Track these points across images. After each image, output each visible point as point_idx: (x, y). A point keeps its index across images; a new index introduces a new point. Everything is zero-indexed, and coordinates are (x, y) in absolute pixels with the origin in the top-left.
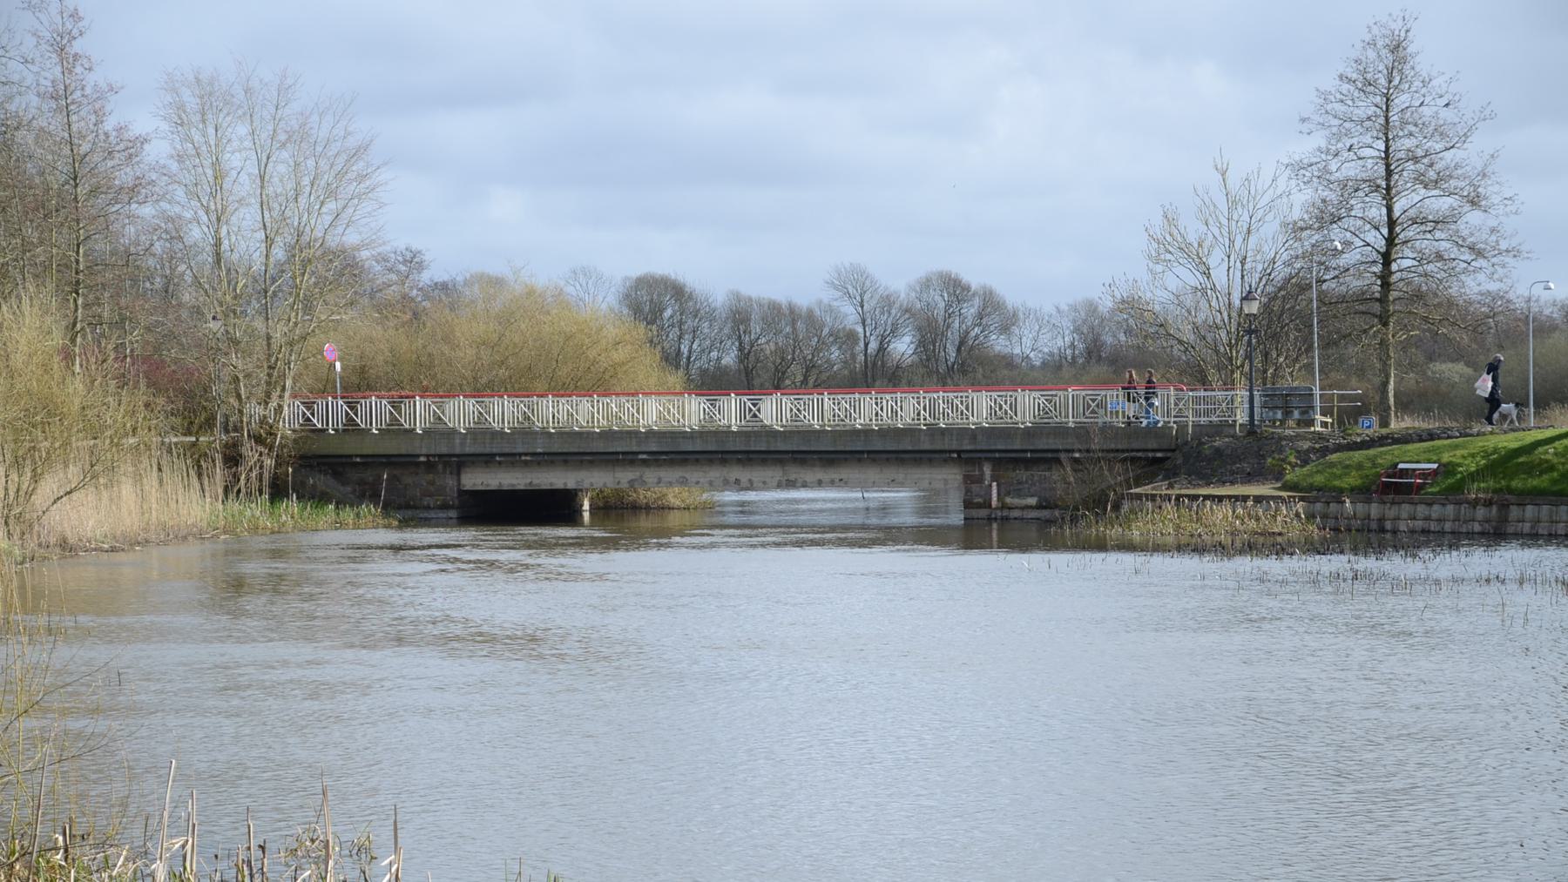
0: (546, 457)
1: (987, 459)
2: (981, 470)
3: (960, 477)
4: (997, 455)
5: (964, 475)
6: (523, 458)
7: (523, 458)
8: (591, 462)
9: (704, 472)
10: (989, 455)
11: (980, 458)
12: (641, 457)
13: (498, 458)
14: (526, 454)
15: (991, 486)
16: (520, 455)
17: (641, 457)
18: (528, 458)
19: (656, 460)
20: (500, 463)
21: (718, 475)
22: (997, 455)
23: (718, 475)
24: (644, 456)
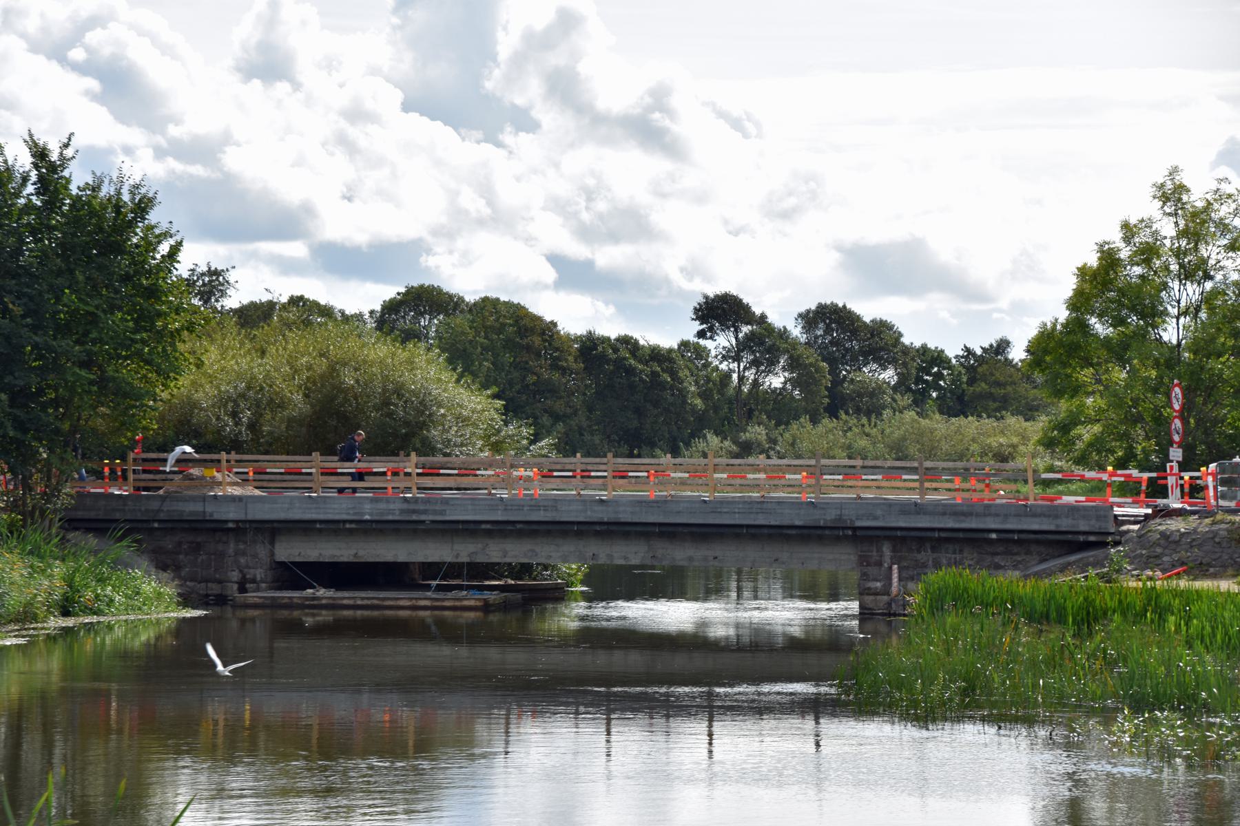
0: (374, 526)
1: (887, 538)
2: (879, 550)
3: (854, 558)
4: (899, 533)
5: (860, 556)
6: (348, 526)
7: (348, 526)
8: (770, 536)
9: (557, 545)
10: (888, 533)
11: (878, 537)
12: (483, 526)
13: (318, 526)
14: (351, 522)
15: (890, 568)
16: (345, 522)
17: (483, 526)
18: (353, 526)
19: (501, 531)
20: (320, 530)
21: (572, 549)
22: (899, 533)
23: (572, 549)
24: (488, 526)
